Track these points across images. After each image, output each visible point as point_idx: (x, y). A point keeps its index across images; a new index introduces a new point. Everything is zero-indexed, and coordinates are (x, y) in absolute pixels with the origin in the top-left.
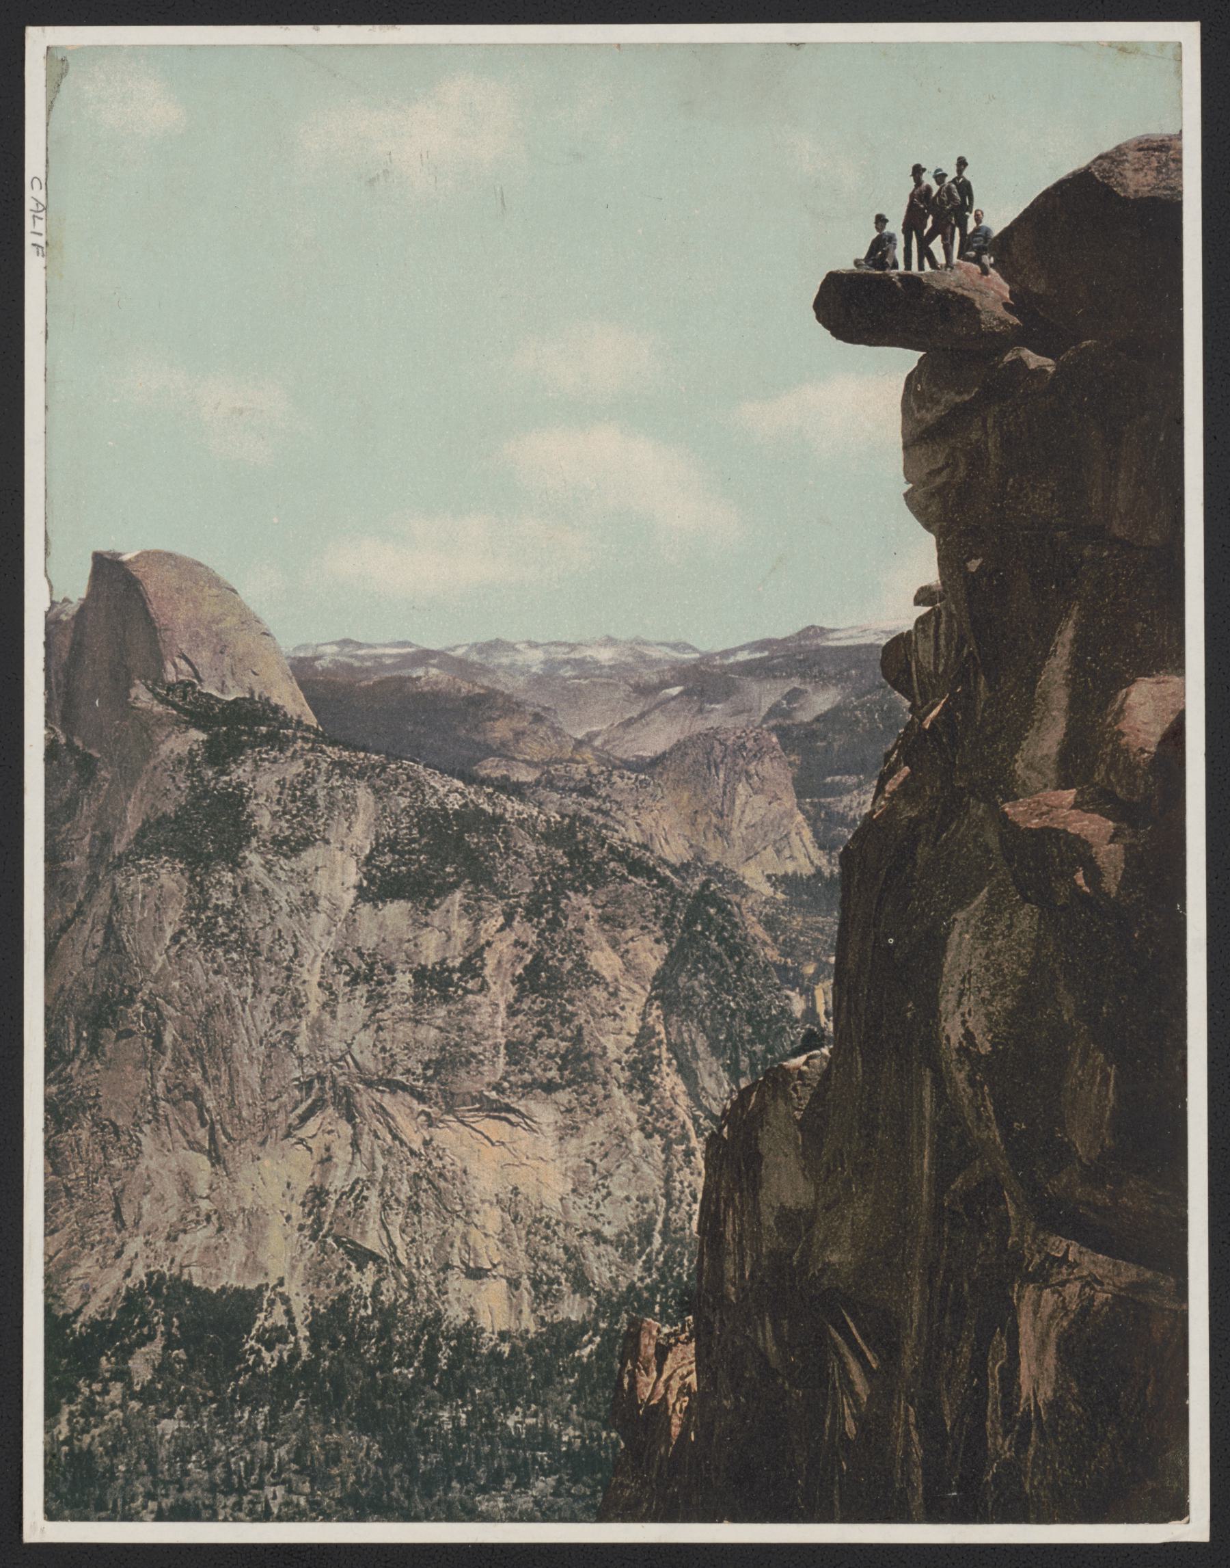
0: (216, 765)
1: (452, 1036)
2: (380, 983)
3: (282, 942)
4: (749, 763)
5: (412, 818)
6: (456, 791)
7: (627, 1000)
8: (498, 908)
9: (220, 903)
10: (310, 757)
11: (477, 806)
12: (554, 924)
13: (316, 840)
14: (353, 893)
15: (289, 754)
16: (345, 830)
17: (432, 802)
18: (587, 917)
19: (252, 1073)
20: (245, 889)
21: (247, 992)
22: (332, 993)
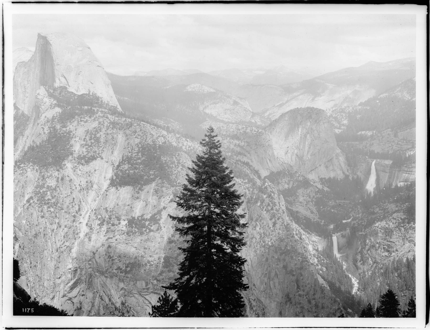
0: (63, 122)
1: (140, 252)
2: (113, 225)
3: (74, 204)
6: (162, 136)
8: (171, 192)
9: (50, 185)
10: (101, 120)
13: (98, 157)
14: (108, 182)
15: (93, 118)
16: (110, 153)
17: (150, 141)
19: (51, 265)
20: (62, 179)
21: (55, 226)
22: (91, 229)
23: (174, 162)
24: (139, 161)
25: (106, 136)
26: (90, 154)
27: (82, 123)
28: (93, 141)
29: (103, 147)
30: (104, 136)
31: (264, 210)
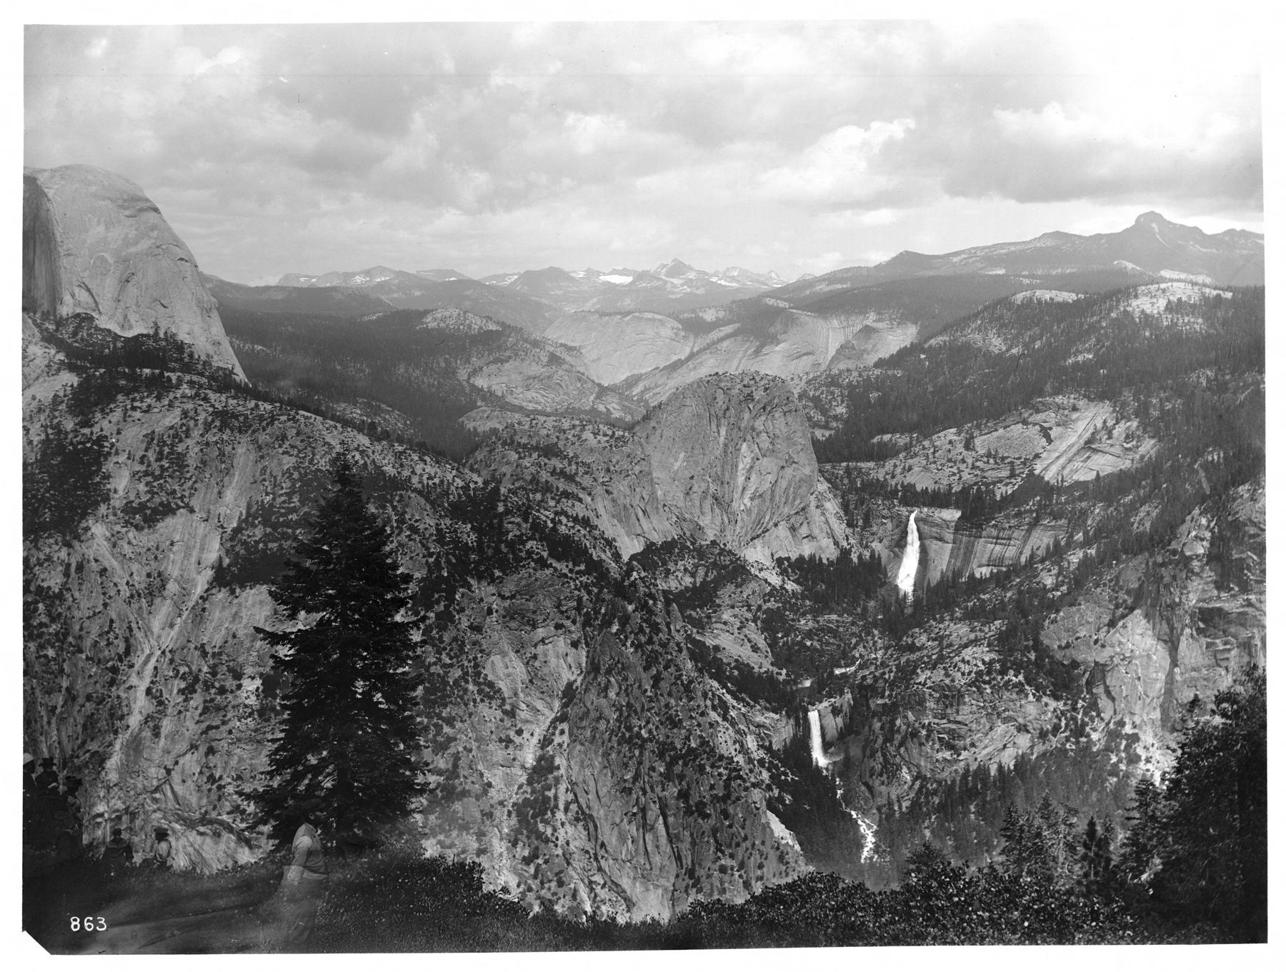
0: (82, 413)
2: (222, 691)
3: (111, 635)
4: (755, 417)
5: (294, 482)
7: (527, 721)
9: (45, 585)
10: (190, 406)
11: (378, 468)
12: (445, 619)
13: (179, 507)
14: (209, 574)
16: (215, 495)
18: (490, 612)
20: (80, 568)
21: (59, 699)
22: (160, 703)
23: (389, 518)
24: (294, 517)
25: (202, 450)
26: (157, 500)
27: (137, 414)
28: (165, 463)
29: (193, 479)
30: (197, 449)
31: (628, 644)
